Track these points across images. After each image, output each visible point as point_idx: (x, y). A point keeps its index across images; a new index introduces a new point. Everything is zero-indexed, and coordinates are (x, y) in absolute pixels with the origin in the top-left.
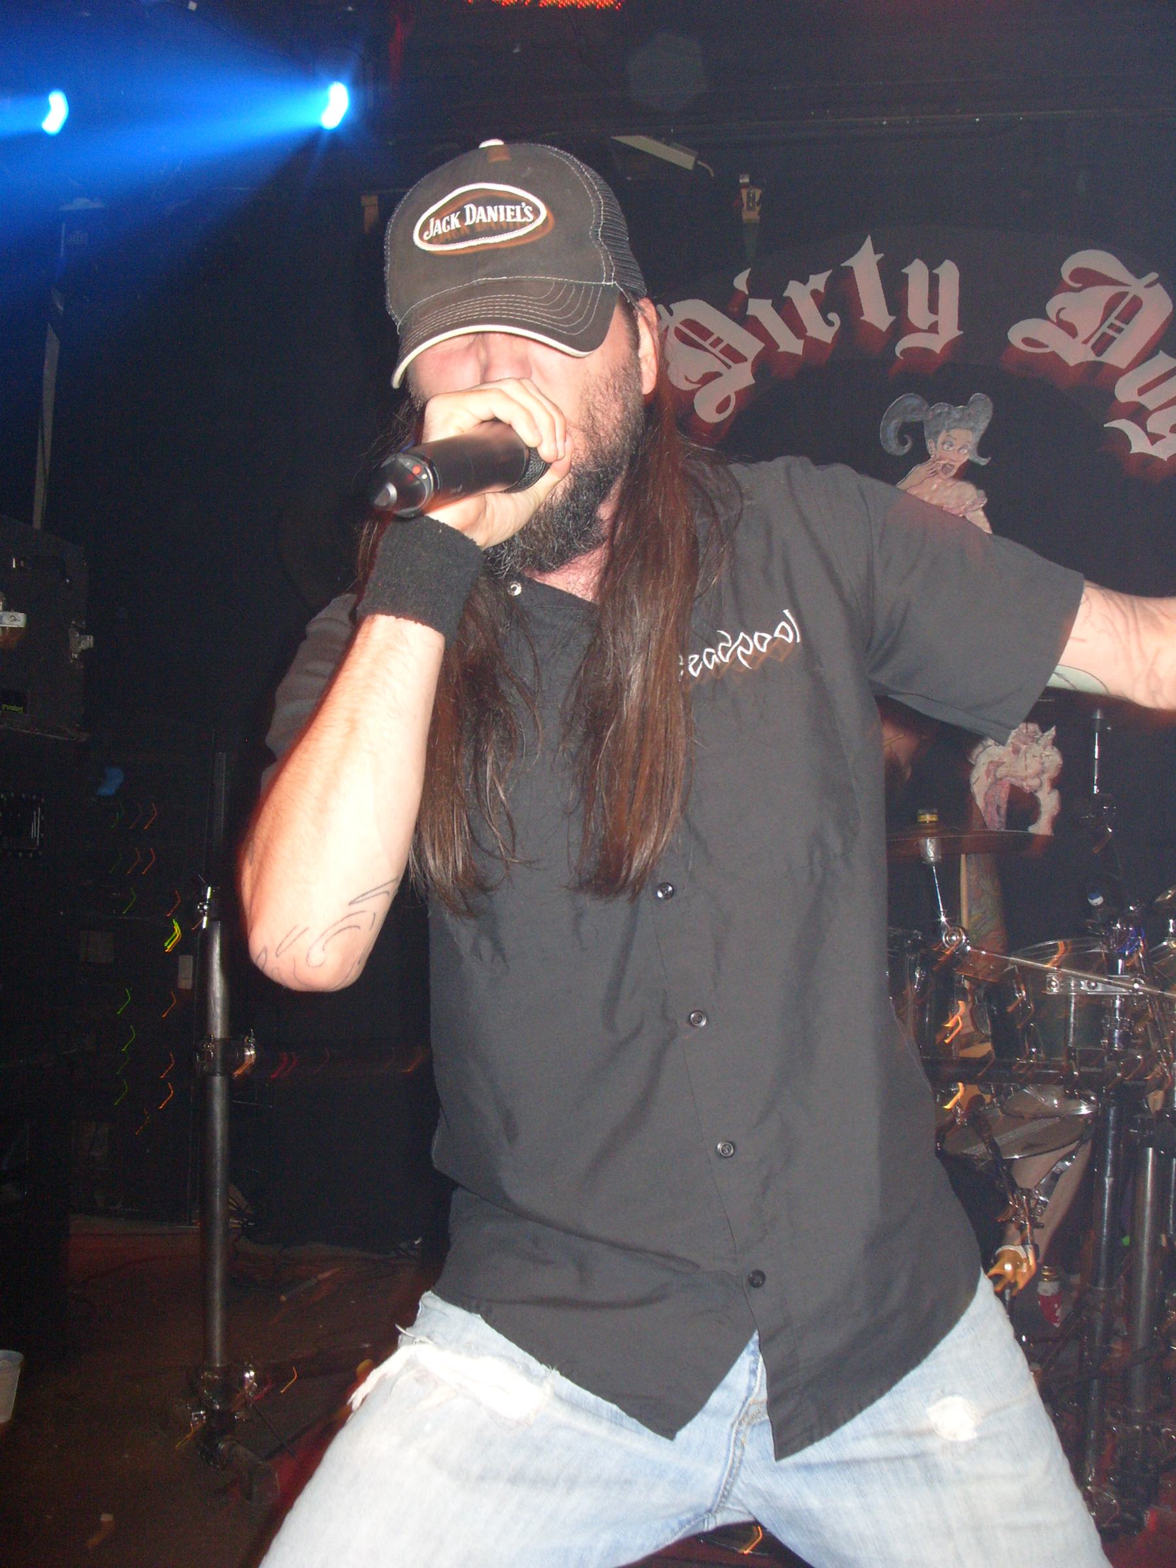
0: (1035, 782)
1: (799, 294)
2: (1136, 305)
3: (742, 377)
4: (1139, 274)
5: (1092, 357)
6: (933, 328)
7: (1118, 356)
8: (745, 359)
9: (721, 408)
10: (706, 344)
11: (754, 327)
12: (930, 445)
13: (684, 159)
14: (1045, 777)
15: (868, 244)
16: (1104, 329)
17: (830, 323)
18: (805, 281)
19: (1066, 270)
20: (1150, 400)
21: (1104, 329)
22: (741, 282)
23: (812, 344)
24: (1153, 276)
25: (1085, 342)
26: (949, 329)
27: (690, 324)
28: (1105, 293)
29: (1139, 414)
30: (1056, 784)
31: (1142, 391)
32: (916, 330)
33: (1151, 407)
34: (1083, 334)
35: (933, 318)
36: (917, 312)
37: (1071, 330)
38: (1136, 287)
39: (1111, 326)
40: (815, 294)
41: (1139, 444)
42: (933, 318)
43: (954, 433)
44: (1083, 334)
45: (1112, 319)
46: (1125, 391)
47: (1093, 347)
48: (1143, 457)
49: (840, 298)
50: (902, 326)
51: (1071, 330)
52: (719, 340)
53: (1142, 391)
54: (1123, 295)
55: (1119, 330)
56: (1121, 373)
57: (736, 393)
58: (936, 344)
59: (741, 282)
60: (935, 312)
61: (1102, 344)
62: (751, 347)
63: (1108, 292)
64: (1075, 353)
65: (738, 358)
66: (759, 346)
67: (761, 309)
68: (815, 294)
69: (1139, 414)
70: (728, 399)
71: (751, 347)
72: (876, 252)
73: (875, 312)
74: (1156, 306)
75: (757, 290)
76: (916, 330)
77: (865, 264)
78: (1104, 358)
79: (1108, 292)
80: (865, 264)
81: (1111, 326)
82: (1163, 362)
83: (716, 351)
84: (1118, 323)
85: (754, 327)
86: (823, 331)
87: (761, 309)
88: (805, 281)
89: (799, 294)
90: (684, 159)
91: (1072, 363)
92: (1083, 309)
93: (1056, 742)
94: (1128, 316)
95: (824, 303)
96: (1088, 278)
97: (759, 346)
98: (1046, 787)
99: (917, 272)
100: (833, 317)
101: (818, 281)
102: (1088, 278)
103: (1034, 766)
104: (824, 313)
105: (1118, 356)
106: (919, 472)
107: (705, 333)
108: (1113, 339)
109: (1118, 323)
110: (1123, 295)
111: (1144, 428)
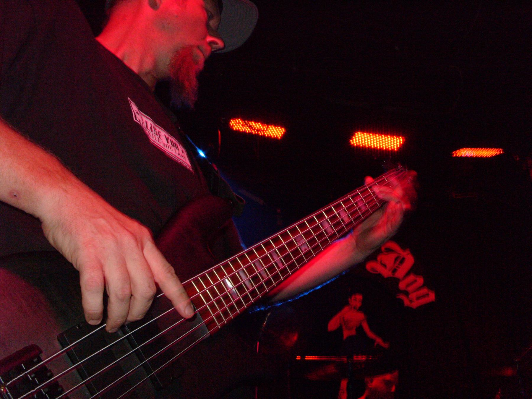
7: (399, 274)
12: (349, 300)
20: (410, 289)
29: (406, 293)
37: (385, 266)
41: (406, 302)
46: (402, 285)
51: (385, 266)
61: (394, 271)
64: (386, 273)
69: (406, 293)
74: (410, 260)
82: (412, 277)
105: (399, 274)
106: (346, 309)
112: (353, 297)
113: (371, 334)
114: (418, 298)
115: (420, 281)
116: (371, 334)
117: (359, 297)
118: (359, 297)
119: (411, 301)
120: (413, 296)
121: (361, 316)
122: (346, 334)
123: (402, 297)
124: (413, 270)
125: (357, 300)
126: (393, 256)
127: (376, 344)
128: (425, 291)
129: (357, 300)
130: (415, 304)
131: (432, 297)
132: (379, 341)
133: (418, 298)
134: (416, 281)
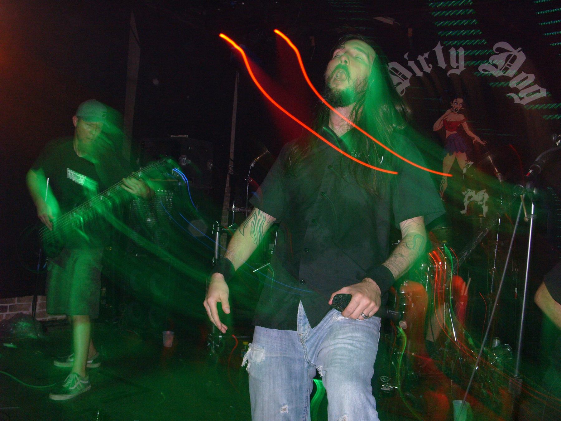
0: (481, 203)
1: (421, 59)
2: (515, 57)
3: (406, 84)
4: (516, 49)
6: (457, 68)
7: (510, 73)
8: (407, 79)
9: (402, 92)
10: (397, 74)
11: (410, 69)
13: (389, 21)
14: (484, 202)
15: (439, 44)
16: (506, 66)
17: (430, 67)
18: (423, 55)
19: (495, 48)
20: (520, 87)
21: (506, 66)
22: (406, 56)
23: (425, 73)
24: (520, 49)
26: (462, 68)
27: (393, 69)
29: (516, 91)
30: (487, 204)
32: (453, 68)
33: (520, 89)
34: (500, 68)
35: (457, 65)
36: (453, 64)
37: (496, 66)
38: (515, 52)
39: (508, 65)
40: (425, 59)
41: (517, 100)
42: (457, 65)
43: (458, 99)
44: (500, 68)
45: (508, 63)
49: (432, 60)
50: (449, 67)
52: (401, 73)
55: (510, 66)
56: (512, 79)
57: (406, 88)
58: (458, 72)
59: (406, 56)
60: (458, 62)
62: (409, 75)
64: (497, 73)
65: (406, 78)
66: (412, 74)
67: (411, 64)
68: (425, 59)
69: (516, 91)
70: (403, 90)
71: (409, 75)
72: (441, 46)
73: (442, 64)
74: (521, 58)
75: (410, 58)
76: (453, 68)
77: (438, 49)
78: (506, 74)
80: (438, 49)
81: (508, 65)
82: (523, 75)
83: (400, 76)
85: (410, 69)
86: (428, 70)
87: (411, 64)
88: (423, 55)
89: (421, 59)
90: (389, 21)
92: (500, 60)
93: (486, 192)
94: (513, 61)
95: (428, 61)
97: (412, 74)
98: (484, 205)
99: (453, 52)
100: (430, 65)
101: (426, 55)
103: (481, 198)
104: (428, 64)
105: (510, 73)
106: (449, 111)
107: (397, 71)
112: (455, 101)
113: (471, 134)
115: (532, 78)
116: (471, 134)
117: (460, 101)
118: (460, 101)
119: (521, 99)
121: (462, 117)
122: (448, 133)
123: (513, 95)
125: (459, 103)
126: (505, 55)
128: (537, 87)
129: (459, 103)
131: (543, 93)
132: (477, 139)
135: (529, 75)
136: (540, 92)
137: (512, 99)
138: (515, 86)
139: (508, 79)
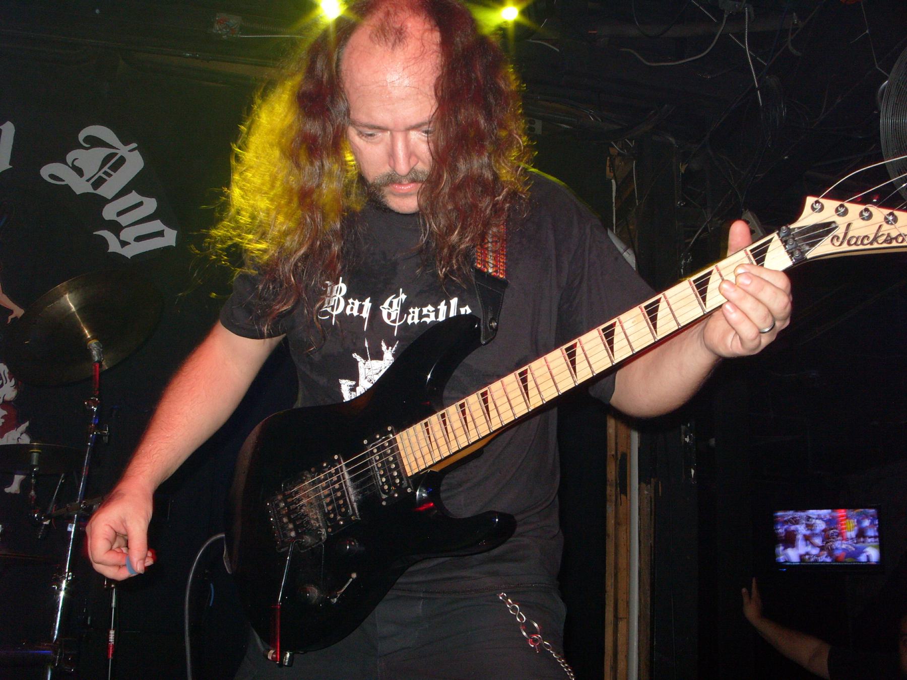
2: (122, 160)
4: (126, 143)
5: (91, 190)
7: (106, 191)
16: (101, 174)
19: (82, 136)
20: (124, 220)
21: (101, 174)
24: (134, 145)
25: (88, 181)
28: (104, 152)
29: (116, 228)
31: (120, 214)
37: (80, 172)
38: (123, 150)
39: (105, 173)
41: (114, 246)
44: (87, 175)
45: (106, 169)
46: (109, 213)
47: (93, 184)
48: (115, 254)
51: (80, 172)
53: (120, 214)
54: (115, 154)
55: (109, 175)
63: (107, 151)
64: (81, 186)
69: (116, 228)
74: (134, 163)
79: (107, 151)
81: (105, 173)
82: (133, 197)
84: (109, 171)
91: (78, 193)
92: (89, 160)
96: (95, 142)
102: (95, 142)
105: (106, 191)
108: (106, 180)
109: (109, 171)
110: (115, 154)
111: (118, 236)
114: (139, 239)
115: (150, 205)
119: (124, 244)
120: (128, 234)
124: (137, 185)
126: (104, 152)
127: (10, 318)
128: (157, 225)
130: (129, 252)
133: (139, 239)
134: (140, 204)
135: (146, 200)
136: (163, 236)
137: (104, 242)
138: (114, 218)
139: (105, 201)
